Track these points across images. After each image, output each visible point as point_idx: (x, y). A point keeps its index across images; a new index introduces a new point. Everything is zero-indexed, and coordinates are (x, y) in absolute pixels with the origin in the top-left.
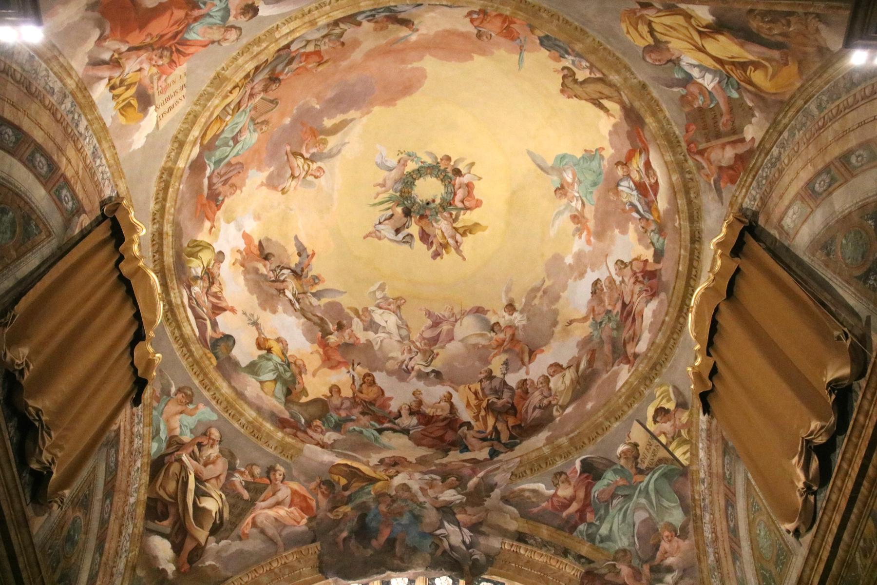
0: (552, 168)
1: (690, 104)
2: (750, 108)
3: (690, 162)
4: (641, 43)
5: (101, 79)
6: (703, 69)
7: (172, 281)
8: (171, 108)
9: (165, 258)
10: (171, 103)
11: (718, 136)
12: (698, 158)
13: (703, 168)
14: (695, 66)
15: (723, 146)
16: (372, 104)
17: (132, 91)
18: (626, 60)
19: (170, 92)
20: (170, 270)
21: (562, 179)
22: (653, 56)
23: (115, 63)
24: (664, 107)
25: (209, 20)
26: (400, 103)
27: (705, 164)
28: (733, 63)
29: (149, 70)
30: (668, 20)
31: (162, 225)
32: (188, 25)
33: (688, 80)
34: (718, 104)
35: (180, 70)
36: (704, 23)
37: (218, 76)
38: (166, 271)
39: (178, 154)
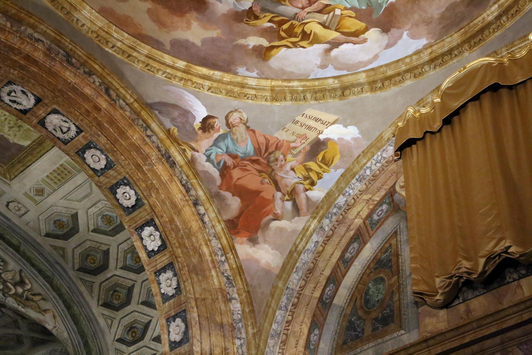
5: (308, 198)
7: (476, 25)
8: (317, 120)
9: (455, 44)
10: (312, 123)
17: (312, 165)
19: (303, 131)
20: (466, 32)
23: (292, 195)
25: (231, 147)
29: (292, 161)
31: (423, 65)
32: (243, 159)
35: (282, 136)
37: (275, 99)
38: (469, 35)
39: (353, 86)
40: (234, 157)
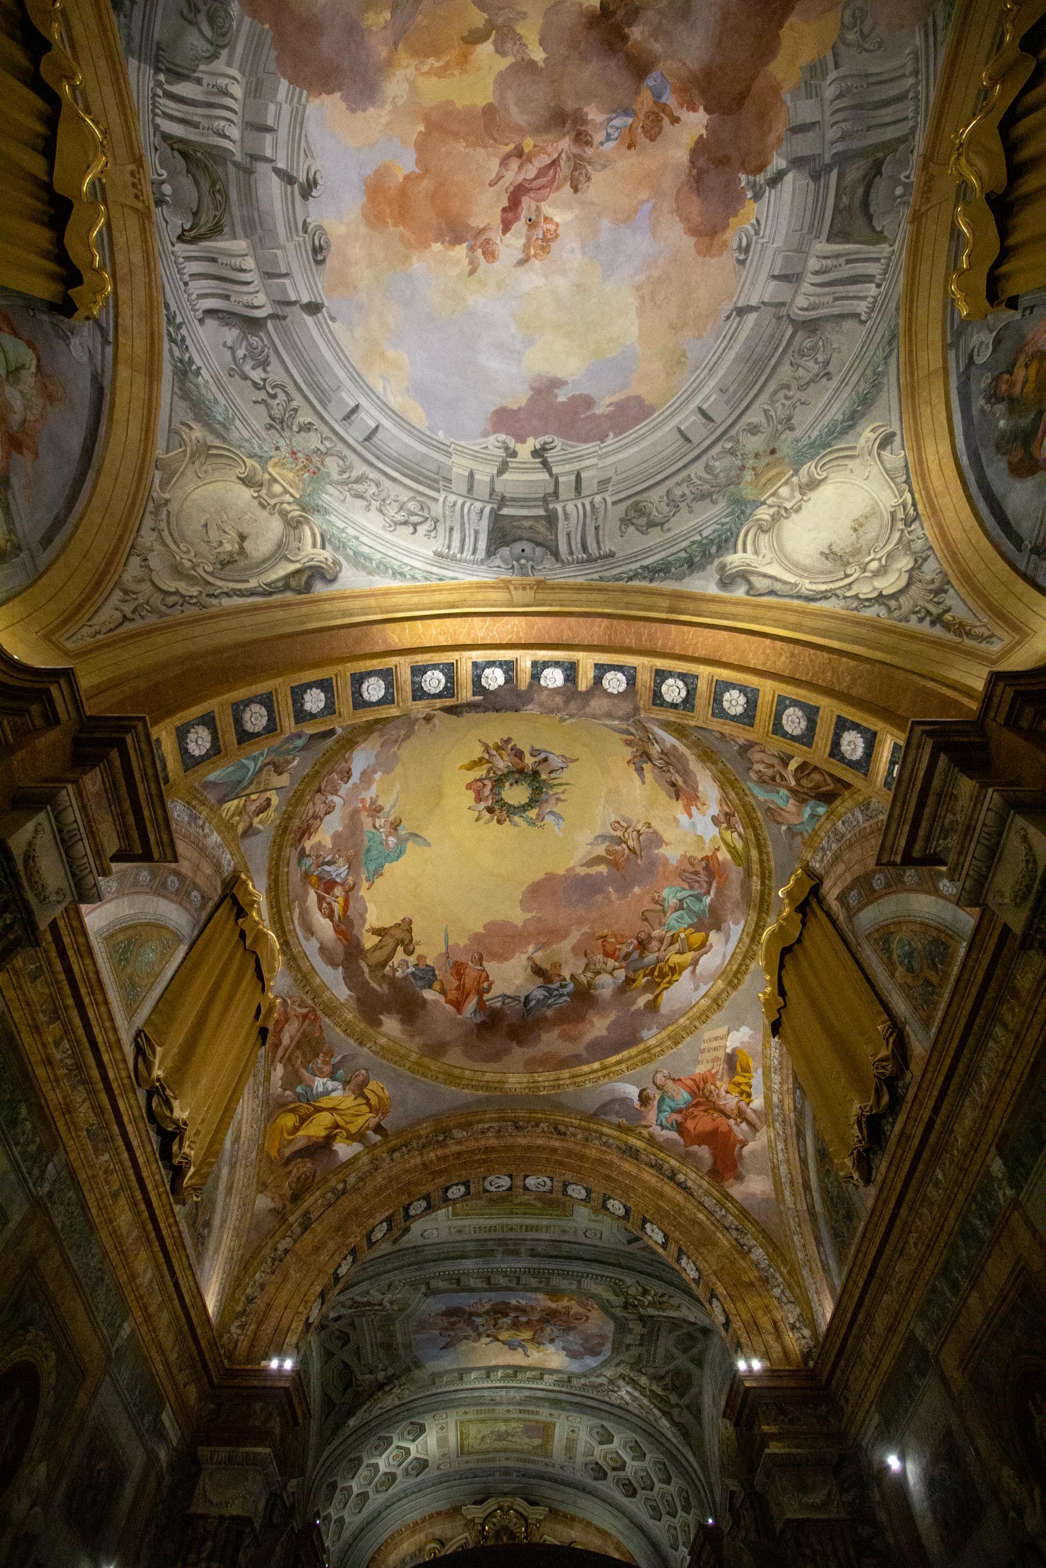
0: (406, 840)
1: (326, 1054)
2: (285, 1089)
3: (310, 1002)
4: (373, 1085)
5: (754, 1111)
6: (327, 1093)
8: (716, 1039)
10: (714, 1044)
11: (298, 1045)
12: (305, 1011)
13: (300, 1006)
14: (333, 1091)
15: (292, 1039)
16: (566, 877)
17: (738, 1079)
18: (379, 1059)
19: (713, 1054)
21: (396, 836)
22: (361, 1078)
23: (741, 1115)
24: (342, 1035)
25: (672, 1104)
26: (542, 876)
27: (299, 1010)
28: (309, 1116)
29: (723, 1085)
30: (361, 1121)
31: (750, 947)
32: (687, 1108)
33: (333, 1078)
34: (306, 1068)
35: (701, 1069)
36: (338, 1138)
37: (676, 1043)
39: (720, 994)
40: (679, 1111)
